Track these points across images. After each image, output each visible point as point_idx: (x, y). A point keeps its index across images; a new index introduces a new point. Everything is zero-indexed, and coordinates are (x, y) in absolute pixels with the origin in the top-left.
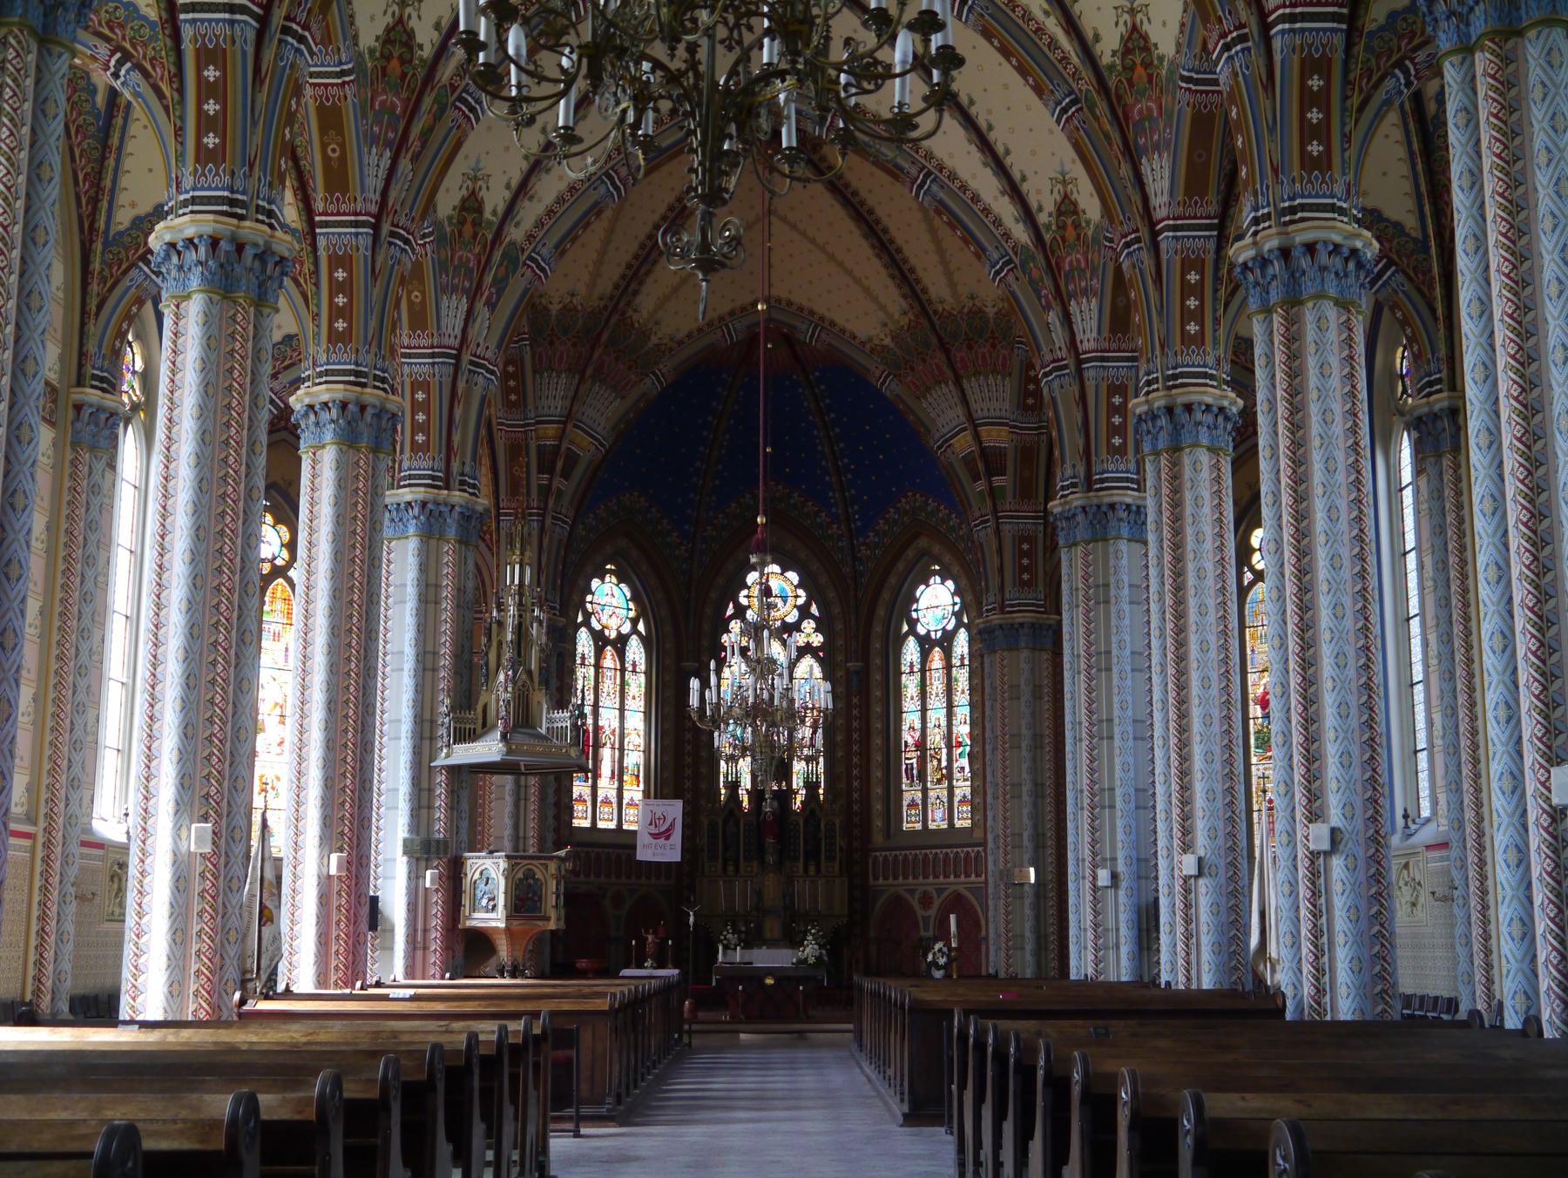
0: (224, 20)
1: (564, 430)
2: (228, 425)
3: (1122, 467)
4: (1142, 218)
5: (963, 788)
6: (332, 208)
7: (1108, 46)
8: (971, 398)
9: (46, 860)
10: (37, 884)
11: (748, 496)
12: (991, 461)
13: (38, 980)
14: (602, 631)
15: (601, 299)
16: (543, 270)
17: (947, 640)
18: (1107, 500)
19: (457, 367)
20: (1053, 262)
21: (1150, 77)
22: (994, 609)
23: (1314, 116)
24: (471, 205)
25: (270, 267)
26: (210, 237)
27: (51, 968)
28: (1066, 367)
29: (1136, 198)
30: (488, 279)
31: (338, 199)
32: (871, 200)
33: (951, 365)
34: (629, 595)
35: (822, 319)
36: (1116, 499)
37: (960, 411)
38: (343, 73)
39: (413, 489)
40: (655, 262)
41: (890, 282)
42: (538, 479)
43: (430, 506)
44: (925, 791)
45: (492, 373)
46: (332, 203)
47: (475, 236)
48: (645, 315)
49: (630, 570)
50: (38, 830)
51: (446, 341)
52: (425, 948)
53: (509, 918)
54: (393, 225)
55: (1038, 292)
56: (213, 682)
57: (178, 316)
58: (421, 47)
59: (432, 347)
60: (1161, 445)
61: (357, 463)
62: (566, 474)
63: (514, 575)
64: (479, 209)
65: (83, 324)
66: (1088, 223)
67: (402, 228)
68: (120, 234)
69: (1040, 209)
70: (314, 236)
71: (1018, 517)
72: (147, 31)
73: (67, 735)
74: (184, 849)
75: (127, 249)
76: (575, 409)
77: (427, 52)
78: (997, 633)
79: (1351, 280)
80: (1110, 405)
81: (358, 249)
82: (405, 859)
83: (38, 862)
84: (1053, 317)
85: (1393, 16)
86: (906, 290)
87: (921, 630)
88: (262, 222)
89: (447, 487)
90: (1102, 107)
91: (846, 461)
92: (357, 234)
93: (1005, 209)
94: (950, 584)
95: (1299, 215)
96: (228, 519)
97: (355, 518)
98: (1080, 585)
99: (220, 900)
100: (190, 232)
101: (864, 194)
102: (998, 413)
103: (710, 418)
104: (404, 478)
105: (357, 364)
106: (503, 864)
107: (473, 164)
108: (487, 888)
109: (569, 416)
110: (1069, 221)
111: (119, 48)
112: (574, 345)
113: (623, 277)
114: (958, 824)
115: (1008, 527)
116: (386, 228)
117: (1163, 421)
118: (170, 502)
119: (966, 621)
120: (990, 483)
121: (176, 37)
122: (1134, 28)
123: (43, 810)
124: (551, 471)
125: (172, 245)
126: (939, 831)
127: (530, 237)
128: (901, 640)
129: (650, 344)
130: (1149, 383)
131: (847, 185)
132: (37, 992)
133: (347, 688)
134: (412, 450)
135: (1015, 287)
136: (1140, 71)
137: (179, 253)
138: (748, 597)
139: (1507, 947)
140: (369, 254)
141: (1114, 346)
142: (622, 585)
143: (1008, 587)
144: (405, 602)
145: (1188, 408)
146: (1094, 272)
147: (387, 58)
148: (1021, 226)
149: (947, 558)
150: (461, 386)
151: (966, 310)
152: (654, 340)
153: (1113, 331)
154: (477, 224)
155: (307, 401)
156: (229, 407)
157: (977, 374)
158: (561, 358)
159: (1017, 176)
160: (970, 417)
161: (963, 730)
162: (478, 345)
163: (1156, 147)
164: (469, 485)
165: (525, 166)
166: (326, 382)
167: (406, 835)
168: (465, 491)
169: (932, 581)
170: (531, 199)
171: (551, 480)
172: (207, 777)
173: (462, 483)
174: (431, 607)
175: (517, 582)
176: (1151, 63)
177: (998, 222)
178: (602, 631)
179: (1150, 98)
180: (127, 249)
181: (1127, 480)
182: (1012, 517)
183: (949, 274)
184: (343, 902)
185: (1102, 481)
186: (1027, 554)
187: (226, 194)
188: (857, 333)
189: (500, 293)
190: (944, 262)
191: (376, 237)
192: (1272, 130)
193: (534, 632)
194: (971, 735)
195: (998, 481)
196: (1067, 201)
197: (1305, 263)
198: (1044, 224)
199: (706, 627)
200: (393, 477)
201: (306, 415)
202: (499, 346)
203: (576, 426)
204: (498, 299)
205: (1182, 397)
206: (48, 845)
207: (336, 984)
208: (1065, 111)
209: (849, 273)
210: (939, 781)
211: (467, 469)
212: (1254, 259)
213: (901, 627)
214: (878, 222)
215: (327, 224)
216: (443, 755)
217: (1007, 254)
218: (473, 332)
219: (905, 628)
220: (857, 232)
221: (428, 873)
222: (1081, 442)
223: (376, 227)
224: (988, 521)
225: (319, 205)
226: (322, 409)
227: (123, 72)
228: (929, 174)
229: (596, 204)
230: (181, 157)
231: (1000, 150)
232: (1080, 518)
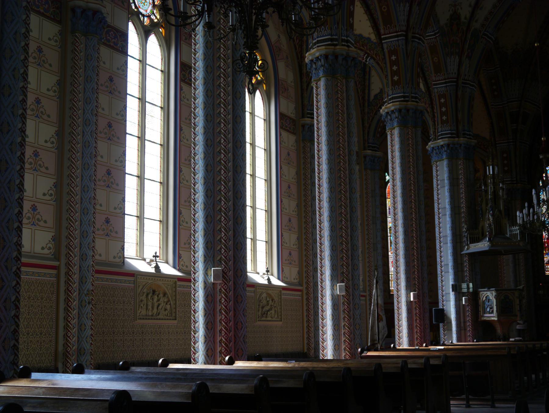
2: (338, 127)
9: (308, 299)
10: (305, 308)
13: (308, 344)
24: (455, 17)
26: (324, 55)
27: (313, 340)
31: (389, 28)
39: (443, 139)
43: (451, 146)
45: (473, 86)
46: (386, 29)
50: (304, 288)
52: (465, 330)
53: (499, 316)
54: (413, 33)
56: (341, 228)
61: (408, 133)
63: (490, 170)
65: (302, 94)
67: (417, 34)
70: (382, 44)
73: (311, 252)
74: (335, 294)
81: (399, 46)
82: (453, 293)
83: (305, 300)
88: (344, 45)
89: (458, 137)
92: (398, 40)
96: (342, 164)
99: (351, 312)
104: (440, 135)
105: (404, 93)
106: (494, 293)
108: (489, 304)
123: (305, 281)
132: (309, 349)
133: (412, 225)
134: (442, 123)
144: (444, 187)
155: (386, 111)
156: (338, 120)
162: (465, 75)
164: (468, 135)
166: (392, 102)
167: (453, 283)
168: (465, 137)
172: (342, 265)
173: (464, 134)
175: (491, 173)
184: (418, 311)
193: (501, 194)
200: (435, 136)
201: (386, 116)
206: (307, 294)
207: (417, 345)
215: (386, 38)
216: (466, 249)
221: (464, 298)
223: (406, 36)
225: (382, 31)
226: (392, 113)
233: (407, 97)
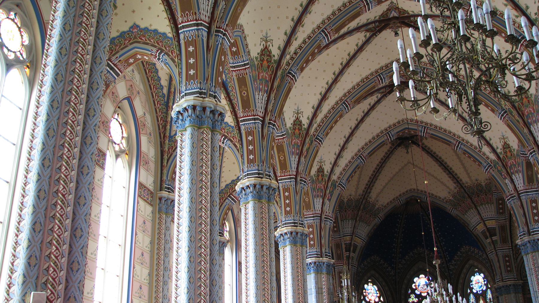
0: (252, 123)
1: (352, 238)
4: (534, 144)
6: (283, 175)
8: (481, 213)
11: (411, 253)
12: (491, 232)
14: (370, 301)
15: (359, 196)
16: (344, 187)
18: (536, 238)
19: (321, 219)
20: (504, 164)
21: (529, 101)
22: (500, 281)
24: (320, 170)
25: (271, 191)
28: (515, 196)
29: (531, 139)
30: (328, 192)
32: (440, 155)
33: (473, 203)
34: (377, 289)
37: (478, 217)
38: (283, 135)
40: (375, 182)
41: (449, 179)
42: (346, 254)
47: (323, 179)
48: (373, 199)
49: (376, 281)
51: (317, 212)
55: (501, 174)
57: (246, 209)
58: (304, 125)
59: (313, 214)
62: (354, 252)
64: (323, 172)
66: (514, 150)
68: (222, 190)
69: (497, 148)
71: (503, 249)
72: (231, 129)
75: (225, 194)
76: (355, 231)
77: (306, 126)
78: (502, 289)
80: (532, 207)
84: (507, 181)
86: (455, 181)
87: (475, 291)
89: (322, 257)
90: (514, 113)
91: (442, 238)
92: (291, 181)
93: (486, 149)
94: (482, 275)
97: (298, 267)
98: (532, 267)
100: (247, 184)
101: (437, 153)
102: (491, 216)
103: (396, 230)
104: (308, 255)
105: (294, 220)
107: (320, 158)
109: (353, 233)
110: (508, 150)
111: (224, 135)
112: (353, 211)
113: (365, 188)
115: (500, 253)
116: (299, 178)
118: (248, 264)
119: (489, 286)
120: (492, 239)
121: (239, 129)
124: (349, 251)
125: (243, 188)
127: (339, 178)
129: (376, 208)
131: (432, 151)
135: (493, 173)
136: (525, 100)
137: (245, 190)
138: (415, 286)
140: (295, 187)
141: (530, 187)
142: (374, 286)
146: (519, 165)
147: (295, 129)
149: (480, 266)
150: (323, 225)
151: (475, 185)
152: (377, 206)
153: (529, 183)
154: (322, 176)
155: (280, 233)
157: (482, 204)
158: (349, 215)
159: (488, 139)
160: (482, 219)
162: (327, 212)
164: (328, 256)
165: (335, 157)
166: (285, 227)
169: (476, 274)
170: (338, 166)
171: (349, 254)
173: (326, 255)
174: (320, 295)
175: (346, 285)
176: (528, 97)
177: (484, 154)
178: (370, 301)
179: (530, 107)
180: (225, 194)
182: (501, 249)
183: (468, 174)
185: (534, 232)
187: (257, 171)
188: (441, 197)
189: (331, 196)
190: (466, 171)
191: (296, 181)
193: (353, 300)
195: (494, 238)
196: (506, 144)
198: (500, 153)
199: (403, 297)
201: (280, 237)
202: (333, 212)
203: (355, 236)
204: (331, 198)
208: (502, 115)
209: (436, 178)
211: (327, 251)
214: (443, 161)
215: (282, 180)
217: (489, 163)
218: (324, 208)
219: (469, 291)
220: (437, 165)
222: (524, 220)
223: (296, 179)
224: (493, 251)
226: (285, 235)
227: (225, 142)
229: (358, 165)
230: (243, 163)
232: (528, 245)
233: (297, 223)
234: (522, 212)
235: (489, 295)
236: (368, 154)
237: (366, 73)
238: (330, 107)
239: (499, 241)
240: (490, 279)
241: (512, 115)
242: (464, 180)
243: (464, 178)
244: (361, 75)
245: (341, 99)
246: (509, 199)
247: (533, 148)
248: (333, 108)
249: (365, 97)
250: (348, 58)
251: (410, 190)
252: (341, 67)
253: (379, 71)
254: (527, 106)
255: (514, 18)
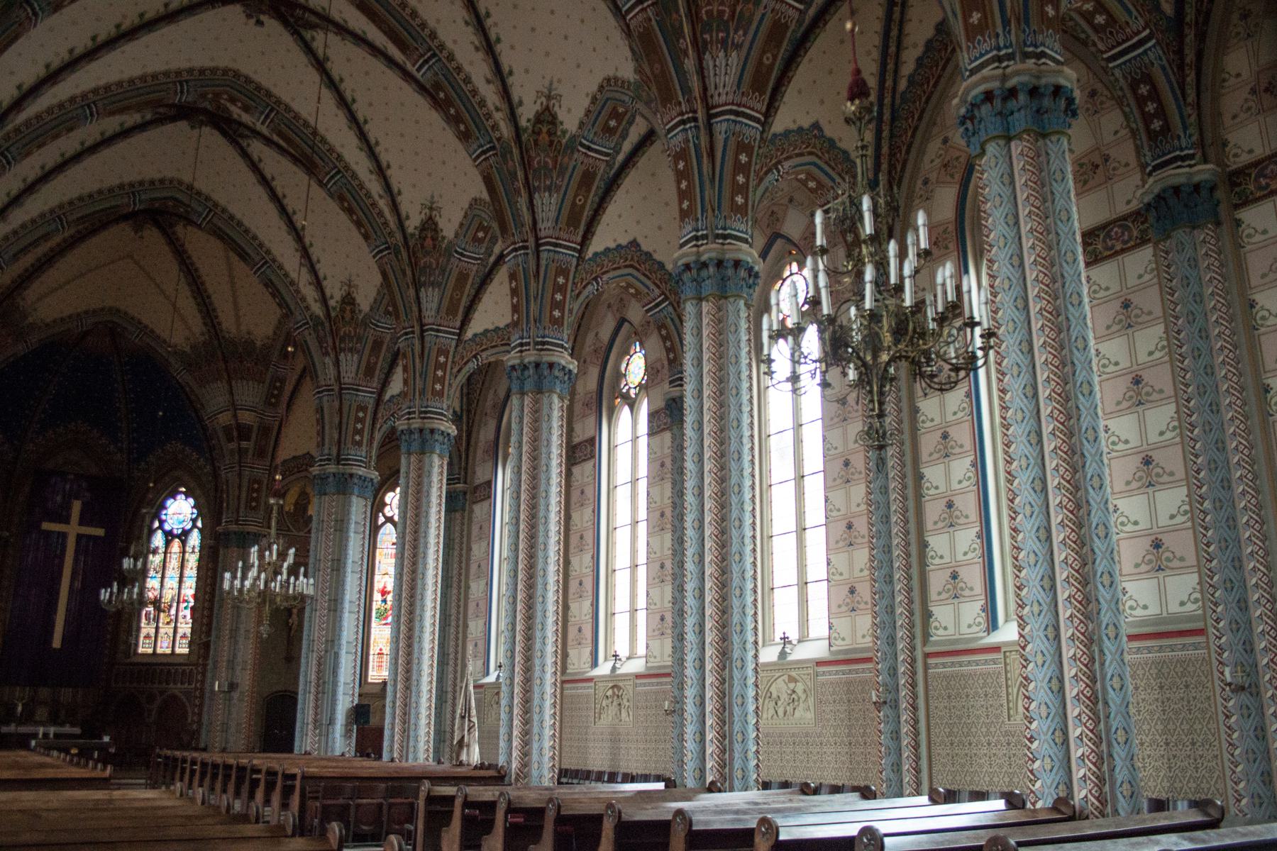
3: (359, 453)
5: (185, 627)
7: (413, 224)
12: (243, 432)
17: (185, 534)
18: (348, 471)
21: (434, 247)
23: (558, 297)
28: (332, 390)
29: (415, 309)
35: (146, 327)
36: (354, 471)
44: (157, 629)
48: (29, 302)
60: (413, 449)
66: (360, 311)
69: (332, 297)
79: (566, 385)
85: (596, 254)
87: (167, 527)
93: (310, 293)
94: (191, 501)
95: (546, 347)
101: (195, 259)
110: (348, 308)
114: (178, 651)
117: (416, 436)
122: (430, 218)
126: (164, 655)
128: (152, 532)
130: (409, 413)
135: (308, 338)
136: (429, 242)
139: (690, 745)
143: (242, 510)
145: (432, 431)
148: (318, 305)
149: (192, 485)
152: (31, 320)
153: (366, 375)
157: (242, 378)
159: (321, 275)
160: (233, 404)
161: (189, 590)
163: (432, 284)
177: (303, 299)
181: (361, 461)
183: (237, 317)
186: (258, 491)
192: (536, 298)
194: (195, 596)
195: (244, 444)
197: (546, 372)
205: (429, 424)
210: (168, 623)
212: (519, 365)
213: (152, 522)
214: (199, 277)
219: (156, 524)
222: (336, 436)
228: (266, 262)
231: (314, 258)
232: (331, 479)
234: (337, 420)
235: (195, 539)
236: (78, 219)
237: (157, 66)
238: (55, 101)
239: (251, 452)
240: (210, 511)
241: (397, 257)
242: (224, 326)
243: (227, 322)
244: (144, 66)
245: (84, 96)
246: (322, 391)
247: (413, 327)
248: (61, 106)
249: (121, 111)
250: (137, 21)
251: (110, 309)
252: (113, 32)
253: (185, 74)
254: (427, 253)
255: (492, 108)
